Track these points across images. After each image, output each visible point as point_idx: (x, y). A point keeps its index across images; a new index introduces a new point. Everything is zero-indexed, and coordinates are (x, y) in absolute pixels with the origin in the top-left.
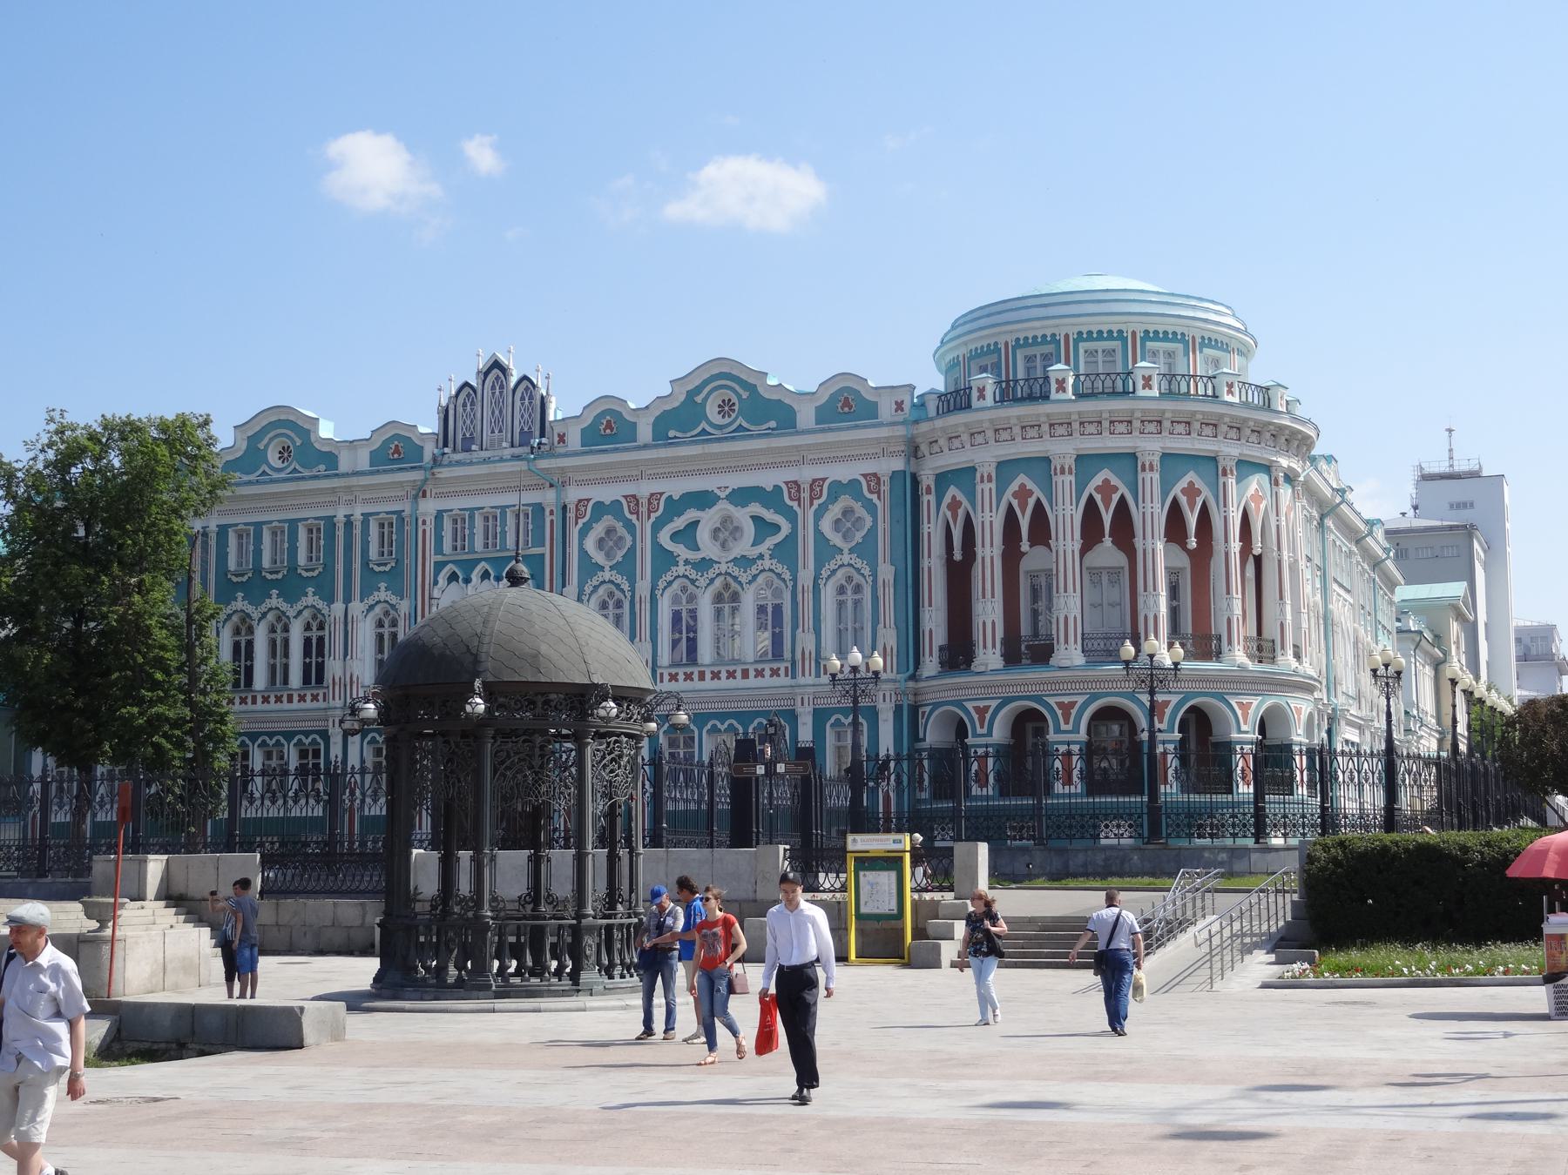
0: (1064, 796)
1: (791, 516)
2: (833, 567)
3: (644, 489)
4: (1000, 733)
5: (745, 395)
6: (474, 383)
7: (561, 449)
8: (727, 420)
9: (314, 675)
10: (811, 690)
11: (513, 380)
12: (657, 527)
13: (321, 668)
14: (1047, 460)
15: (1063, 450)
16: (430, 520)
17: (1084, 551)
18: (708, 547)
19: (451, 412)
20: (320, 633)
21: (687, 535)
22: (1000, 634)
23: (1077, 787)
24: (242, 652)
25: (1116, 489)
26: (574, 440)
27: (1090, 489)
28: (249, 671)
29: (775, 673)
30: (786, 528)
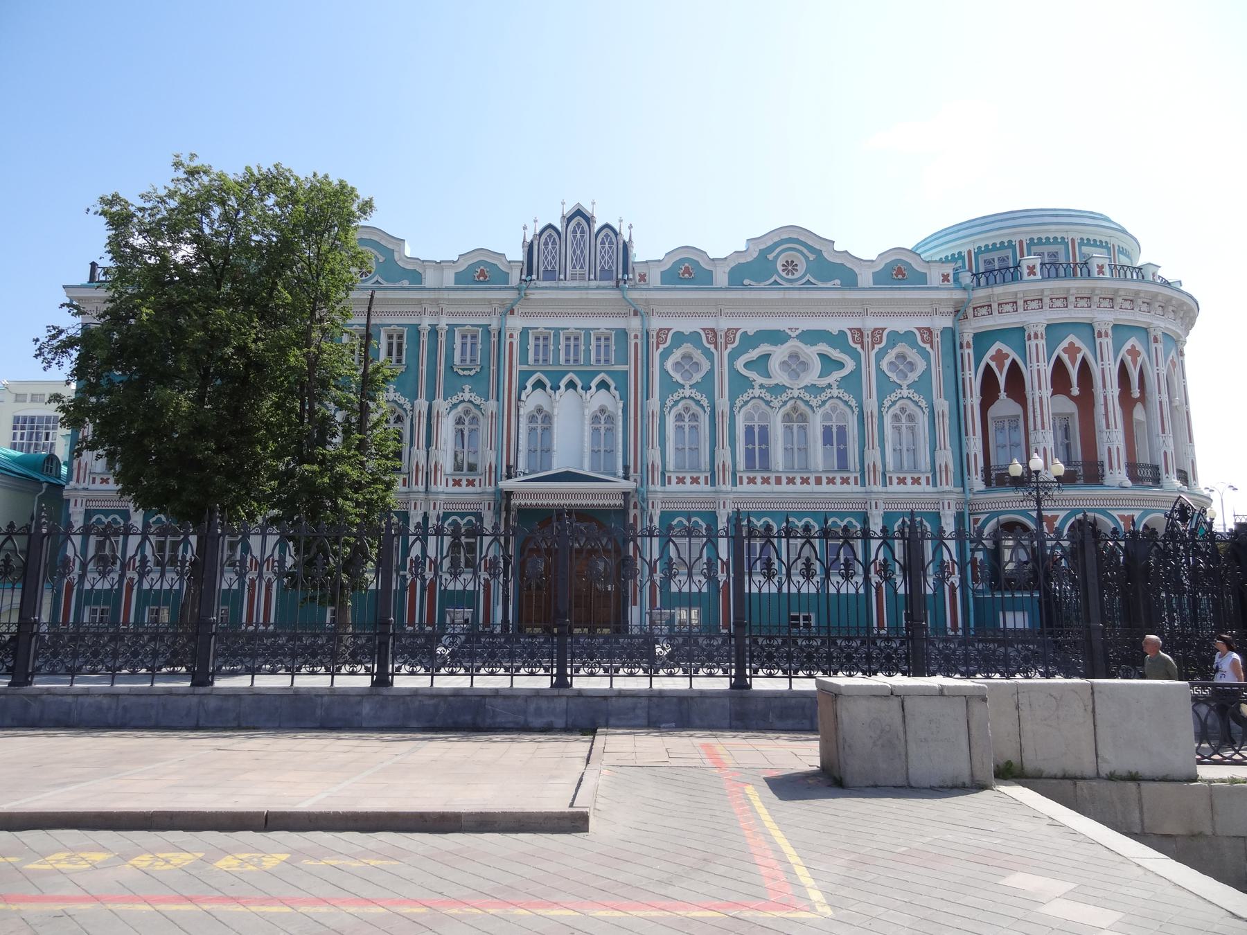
2: (894, 399)
3: (724, 324)
5: (812, 257)
6: (559, 226)
7: (642, 285)
10: (884, 496)
11: (597, 227)
12: (733, 357)
16: (516, 334)
18: (780, 376)
19: (535, 248)
20: (398, 426)
21: (761, 364)
26: (655, 278)
29: (845, 481)
30: (850, 365)
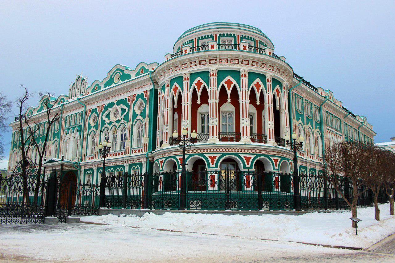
0: (211, 191)
14: (208, 72)
15: (213, 68)
17: (221, 104)
23: (216, 188)
25: (232, 83)
27: (223, 82)
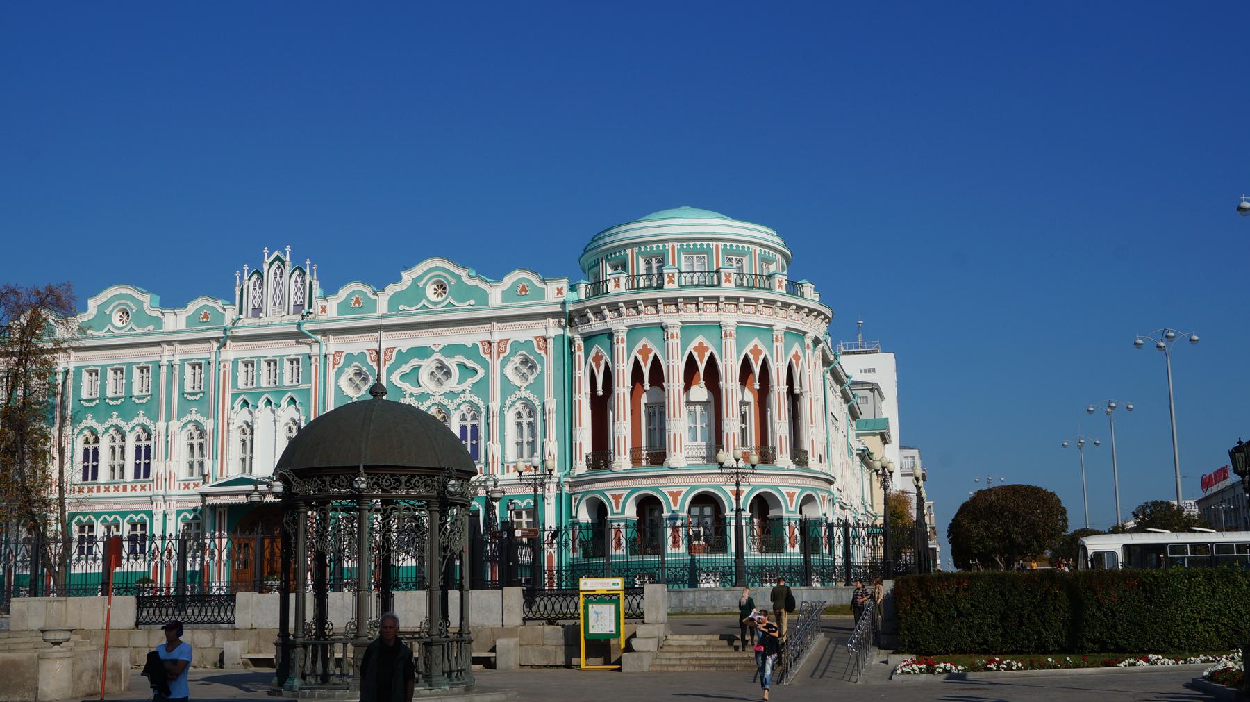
1: (485, 364)
4: (631, 512)
8: (440, 299)
9: (143, 471)
13: (147, 466)
16: (229, 366)
22: (629, 446)
24: (91, 456)
25: (707, 349)
28: (95, 469)
